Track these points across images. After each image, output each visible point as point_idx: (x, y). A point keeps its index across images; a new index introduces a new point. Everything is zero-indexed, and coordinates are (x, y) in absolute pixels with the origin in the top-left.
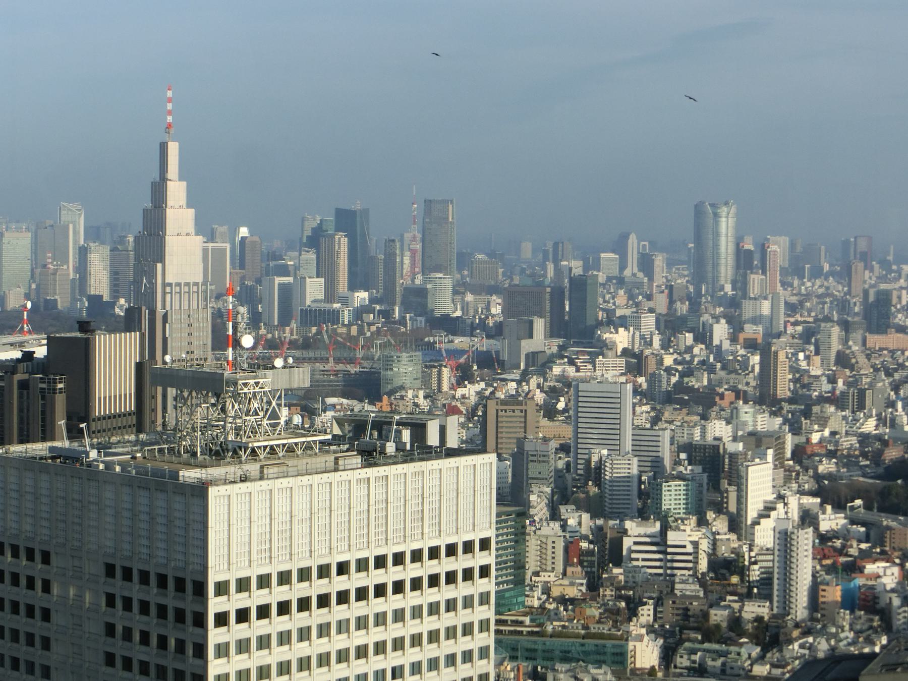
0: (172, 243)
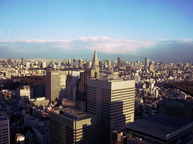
0: (96, 61)
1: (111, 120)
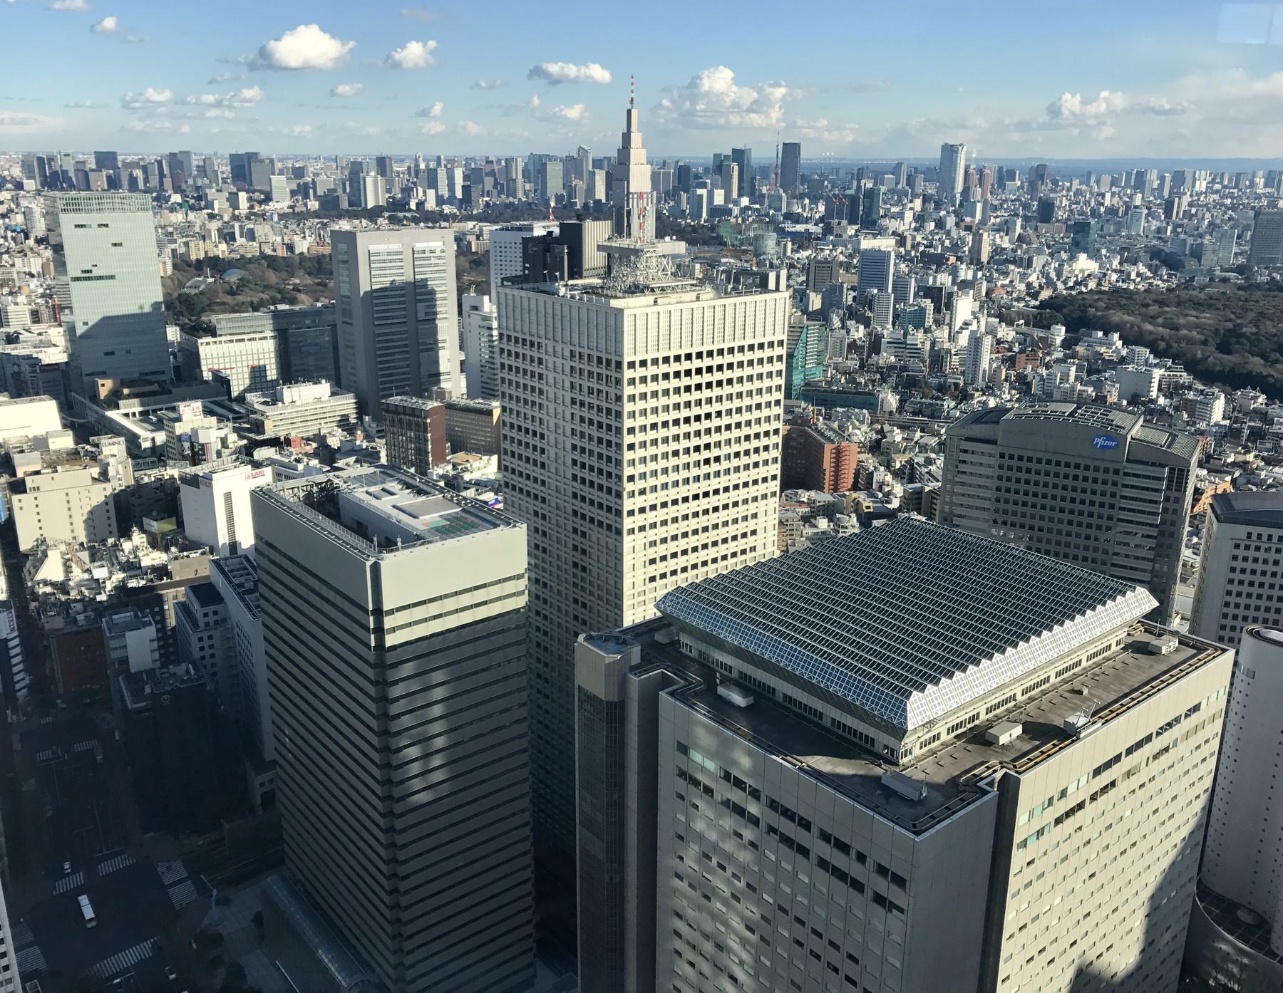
0: (634, 169)
1: (628, 541)
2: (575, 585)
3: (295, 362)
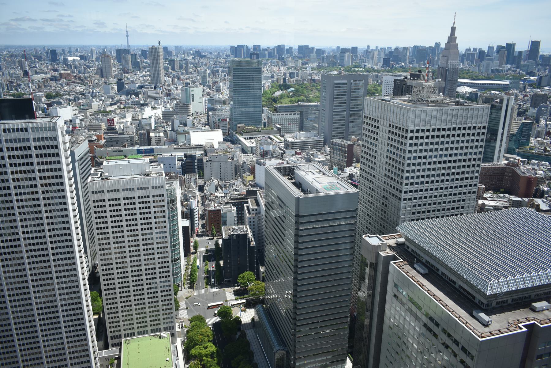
1: (403, 202)
2: (381, 218)
3: (305, 122)
